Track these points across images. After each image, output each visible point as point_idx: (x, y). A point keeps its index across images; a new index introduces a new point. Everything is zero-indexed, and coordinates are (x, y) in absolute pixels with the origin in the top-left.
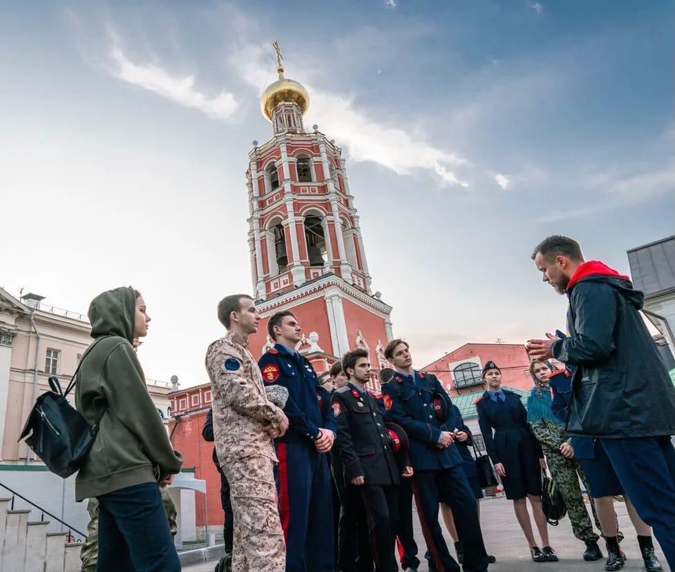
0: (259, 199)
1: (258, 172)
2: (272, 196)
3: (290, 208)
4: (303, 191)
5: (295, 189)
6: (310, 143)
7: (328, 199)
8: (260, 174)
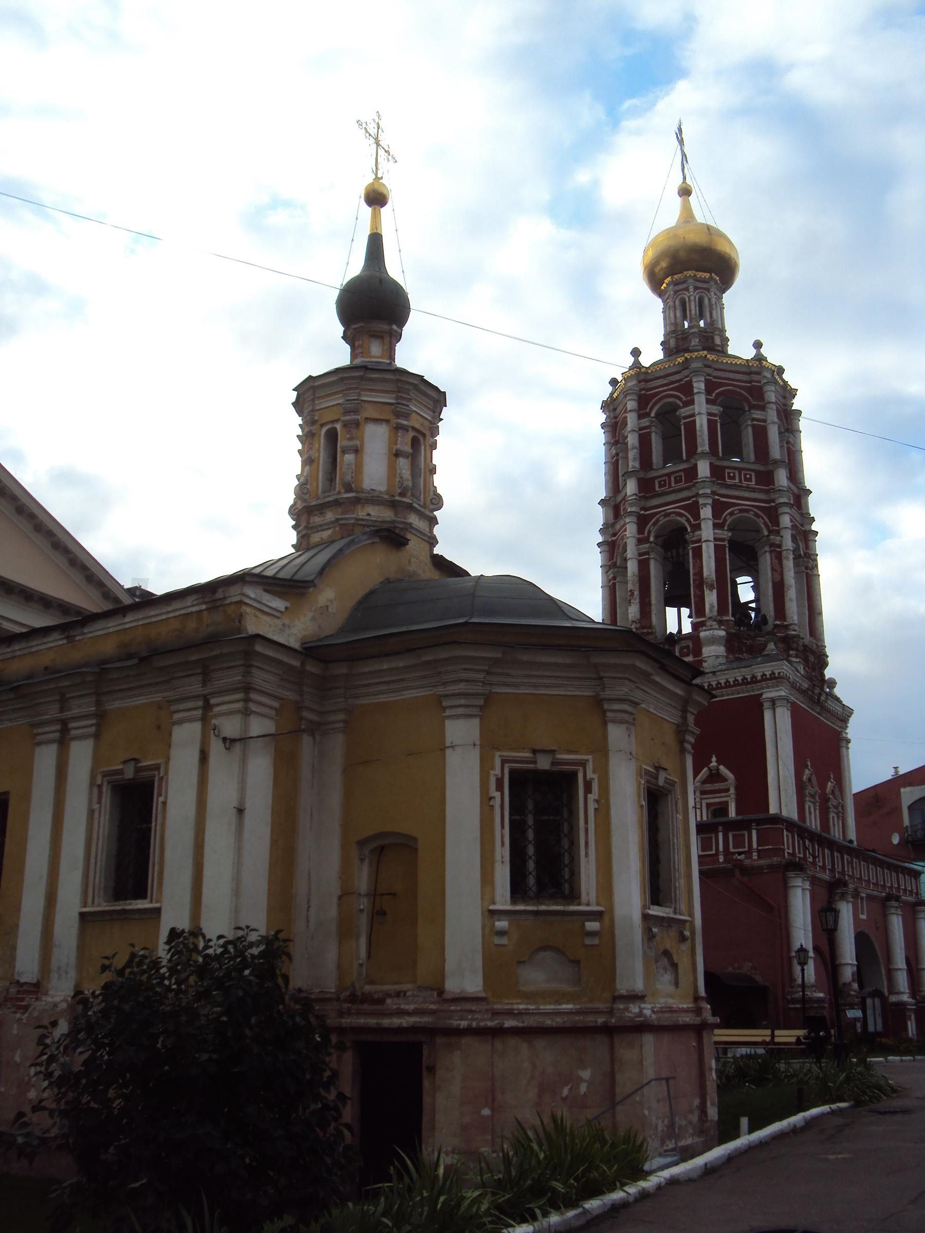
0: (642, 475)
1: (640, 417)
2: (669, 475)
3: (706, 512)
4: (730, 478)
5: (717, 472)
6: (745, 378)
7: (773, 501)
8: (645, 422)
